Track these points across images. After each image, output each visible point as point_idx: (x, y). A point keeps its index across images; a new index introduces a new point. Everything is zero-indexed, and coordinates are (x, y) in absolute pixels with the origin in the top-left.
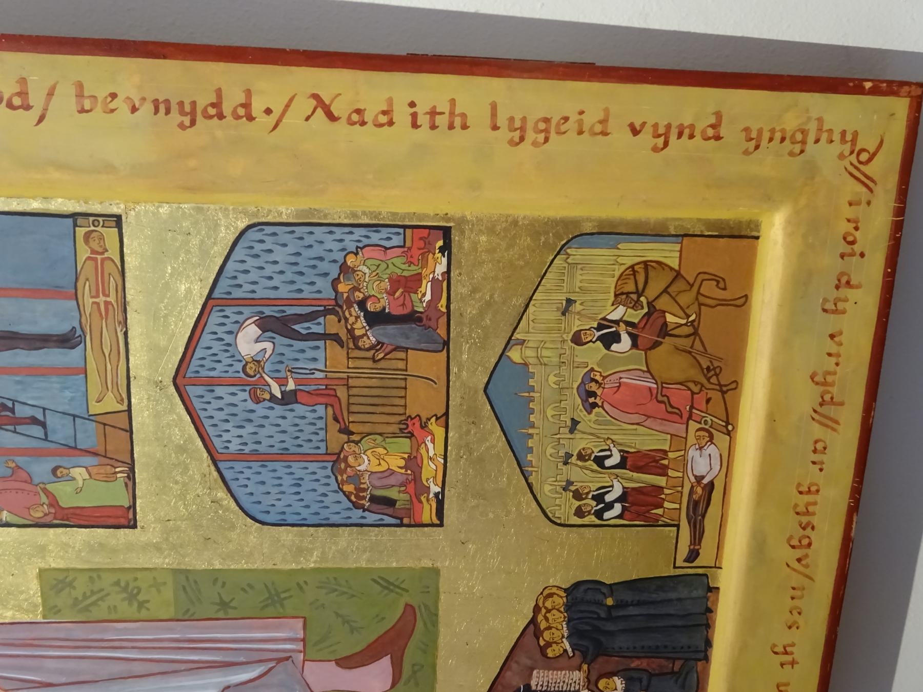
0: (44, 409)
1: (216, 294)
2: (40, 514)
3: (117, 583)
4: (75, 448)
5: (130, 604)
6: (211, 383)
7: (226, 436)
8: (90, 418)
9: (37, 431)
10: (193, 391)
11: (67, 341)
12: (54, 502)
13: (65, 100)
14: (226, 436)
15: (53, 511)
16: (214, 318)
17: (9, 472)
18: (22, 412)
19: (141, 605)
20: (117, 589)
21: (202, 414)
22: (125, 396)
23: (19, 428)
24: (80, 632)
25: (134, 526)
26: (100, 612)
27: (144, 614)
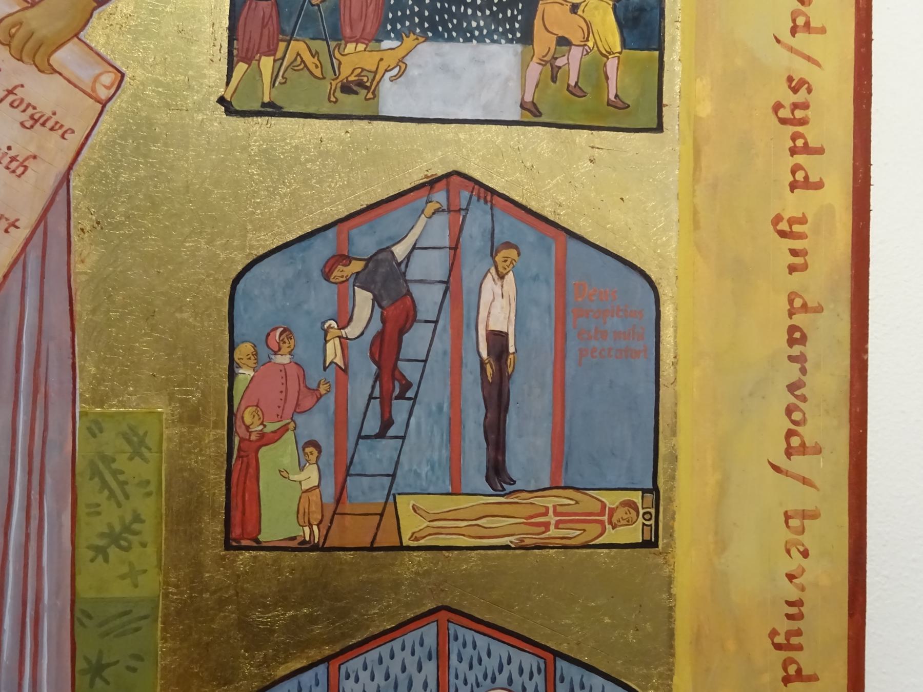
0: (403, 438)
1: (560, 663)
2: (248, 420)
3: (137, 519)
4: (348, 474)
5: (102, 535)
6: (441, 656)
7: (364, 676)
8: (391, 497)
9: (372, 425)
10: (429, 632)
11: (497, 473)
12: (266, 439)
13: (805, 499)
14: (364, 676)
15: (254, 437)
16: (529, 661)
17: (314, 386)
18: (400, 409)
19: (101, 551)
20: (128, 518)
21: (397, 645)
22: (422, 542)
23: (376, 404)
24: (57, 461)
25: (228, 547)
26: (89, 492)
27: (85, 554)
